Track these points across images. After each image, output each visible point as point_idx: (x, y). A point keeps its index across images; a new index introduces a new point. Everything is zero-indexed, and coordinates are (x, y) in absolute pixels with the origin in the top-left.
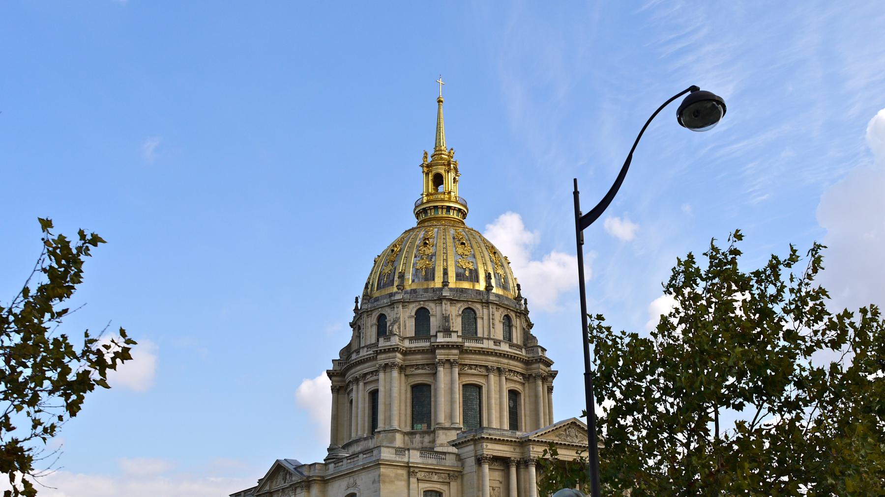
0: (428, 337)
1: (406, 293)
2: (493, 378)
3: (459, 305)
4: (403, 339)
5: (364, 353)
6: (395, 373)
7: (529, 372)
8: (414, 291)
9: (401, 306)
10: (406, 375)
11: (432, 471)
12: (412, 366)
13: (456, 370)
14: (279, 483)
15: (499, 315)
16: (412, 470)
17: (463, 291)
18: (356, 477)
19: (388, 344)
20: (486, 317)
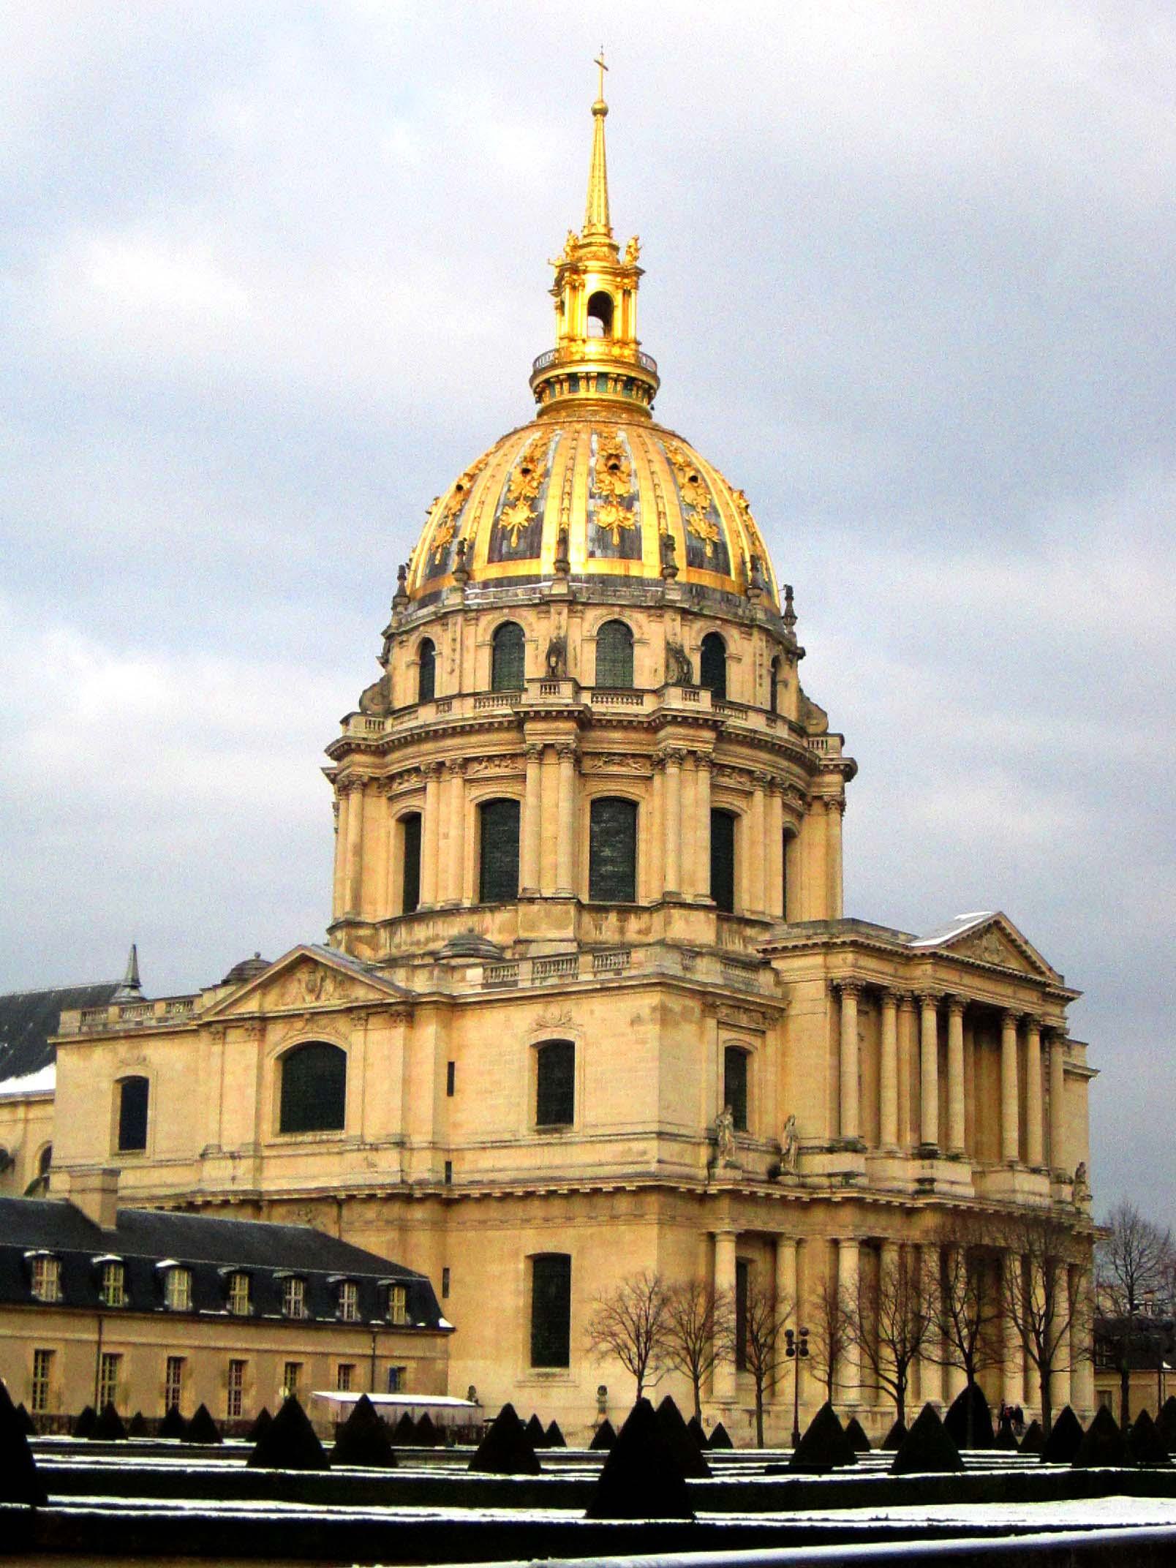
0: (639, 695)
1: (576, 579)
3: (699, 625)
4: (578, 689)
5: (464, 711)
6: (566, 769)
7: (814, 791)
9: (566, 611)
10: (581, 775)
11: (739, 1006)
12: (597, 755)
13: (704, 776)
14: (296, 996)
16: (710, 999)
18: (569, 1005)
20: (747, 660)
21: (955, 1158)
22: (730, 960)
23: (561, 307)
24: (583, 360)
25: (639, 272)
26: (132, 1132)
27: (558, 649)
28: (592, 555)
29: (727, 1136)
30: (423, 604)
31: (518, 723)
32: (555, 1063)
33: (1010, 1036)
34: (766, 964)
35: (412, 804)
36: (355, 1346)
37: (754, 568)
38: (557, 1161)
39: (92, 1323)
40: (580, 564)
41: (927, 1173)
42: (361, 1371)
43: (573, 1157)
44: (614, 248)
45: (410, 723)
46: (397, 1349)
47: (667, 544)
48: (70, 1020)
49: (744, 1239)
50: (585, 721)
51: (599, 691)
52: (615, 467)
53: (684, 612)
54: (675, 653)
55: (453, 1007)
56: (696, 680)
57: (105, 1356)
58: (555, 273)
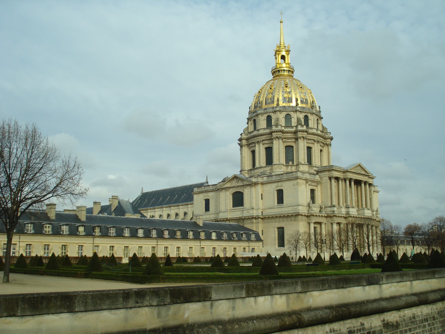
1: (281, 107)
2: (316, 144)
4: (282, 127)
5: (261, 132)
6: (281, 141)
7: (326, 143)
8: (284, 107)
11: (313, 181)
12: (286, 138)
13: (305, 141)
14: (234, 183)
15: (316, 118)
17: (303, 108)
19: (277, 129)
22: (311, 174)
23: (276, 58)
24: (280, 68)
25: (290, 51)
26: (207, 209)
27: (278, 120)
28: (283, 102)
29: (311, 205)
30: (254, 113)
31: (271, 133)
32: (280, 193)
33: (363, 185)
34: (317, 174)
35: (253, 149)
36: (245, 244)
37: (313, 103)
38: (281, 211)
39: (199, 242)
40: (281, 104)
41: (348, 211)
42: (247, 248)
44: (285, 47)
45: (252, 134)
46: (253, 245)
47: (297, 100)
48: (196, 190)
50: (283, 132)
51: (285, 127)
52: (287, 86)
54: (298, 120)
55: (262, 184)
56: (303, 124)
58: (274, 52)
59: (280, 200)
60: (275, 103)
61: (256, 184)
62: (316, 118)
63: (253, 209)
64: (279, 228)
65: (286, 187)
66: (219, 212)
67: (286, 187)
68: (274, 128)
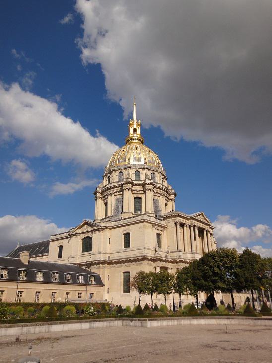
3: (151, 171)
5: (113, 185)
6: (130, 191)
7: (170, 198)
21: (197, 253)
26: (60, 255)
27: (128, 174)
29: (157, 249)
32: (127, 236)
33: (205, 233)
36: (83, 288)
38: (126, 254)
41: (193, 256)
43: (131, 253)
47: (145, 159)
49: (161, 268)
52: (137, 149)
53: (148, 169)
54: (147, 175)
57: (19, 292)
59: (127, 244)
60: (127, 161)
61: (105, 228)
62: (162, 177)
63: (100, 253)
64: (124, 273)
65: (133, 230)
66: (69, 258)
67: (133, 230)
68: (124, 181)
